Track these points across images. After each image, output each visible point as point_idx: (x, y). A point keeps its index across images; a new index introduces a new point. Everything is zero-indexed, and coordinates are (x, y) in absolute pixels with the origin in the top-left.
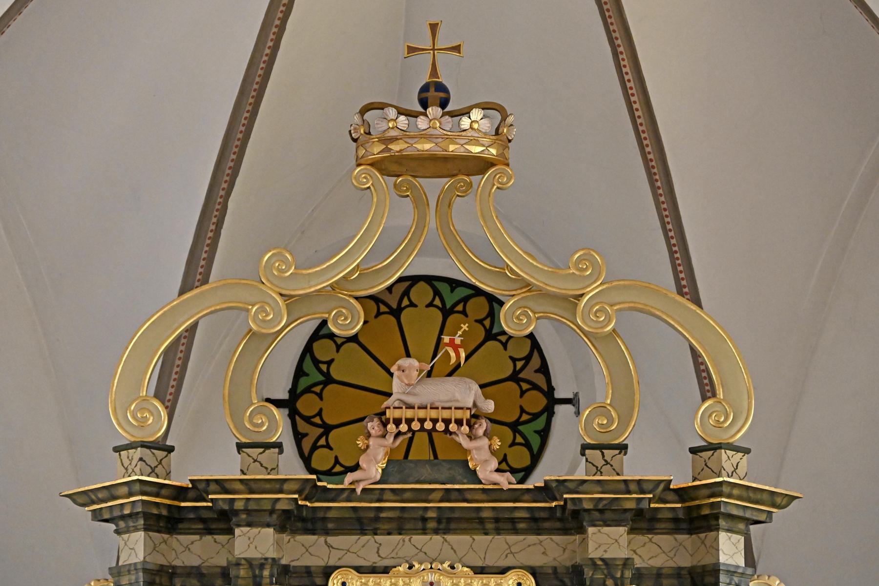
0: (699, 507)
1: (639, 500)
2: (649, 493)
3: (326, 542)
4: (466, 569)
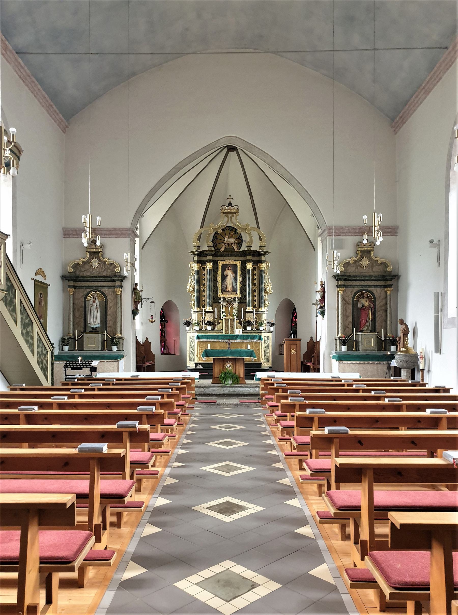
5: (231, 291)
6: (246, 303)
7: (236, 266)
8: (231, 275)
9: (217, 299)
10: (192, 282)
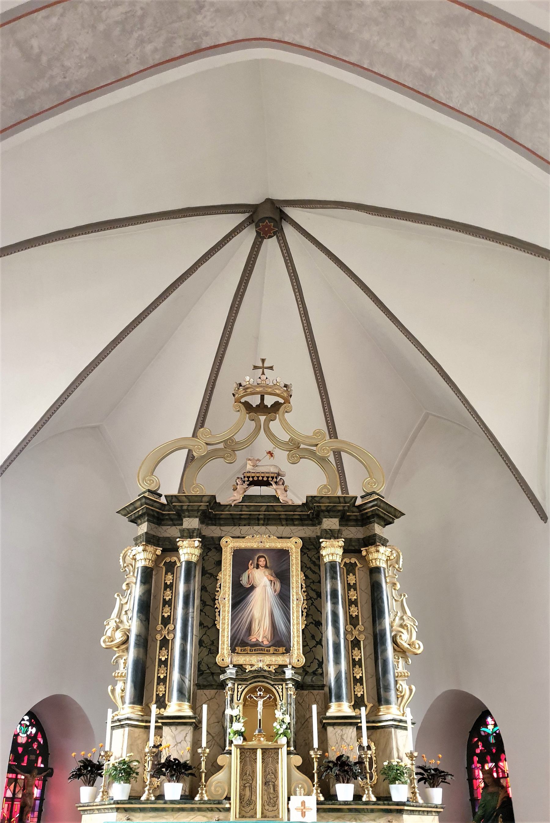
0: (367, 513)
1: (344, 506)
2: (348, 503)
3: (220, 529)
4: (275, 537)
5: (266, 643)
6: (326, 689)
7: (284, 554)
8: (265, 586)
9: (213, 674)
10: (123, 612)
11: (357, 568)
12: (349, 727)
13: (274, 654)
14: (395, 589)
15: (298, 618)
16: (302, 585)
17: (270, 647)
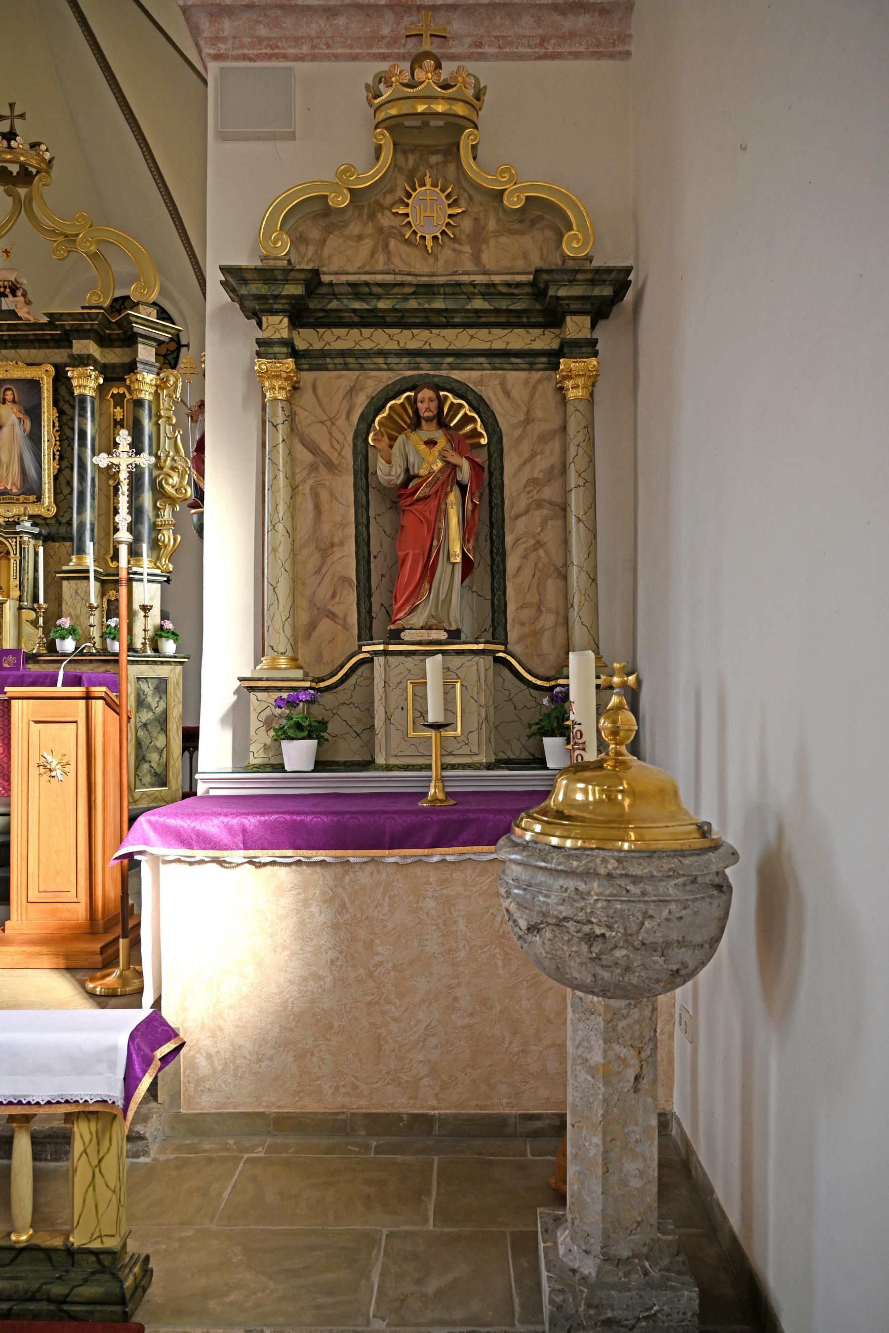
5: (15, 490)
7: (34, 385)
8: (13, 425)
11: (126, 400)
12: (84, 581)
13: (24, 503)
14: (169, 425)
15: (49, 462)
16: (54, 423)
17: (19, 495)
